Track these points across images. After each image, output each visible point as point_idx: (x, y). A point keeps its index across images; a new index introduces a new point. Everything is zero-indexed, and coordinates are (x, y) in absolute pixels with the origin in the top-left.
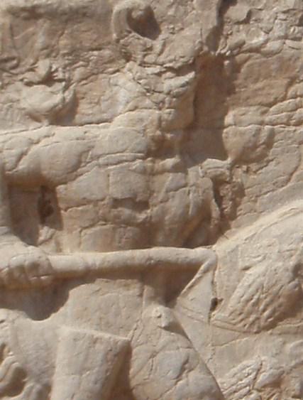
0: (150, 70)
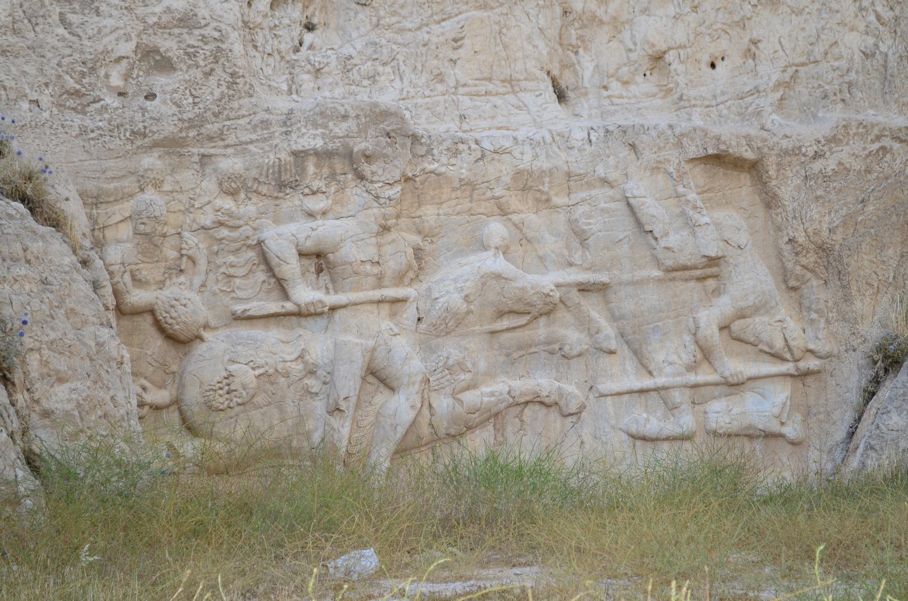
0: (376, 185)
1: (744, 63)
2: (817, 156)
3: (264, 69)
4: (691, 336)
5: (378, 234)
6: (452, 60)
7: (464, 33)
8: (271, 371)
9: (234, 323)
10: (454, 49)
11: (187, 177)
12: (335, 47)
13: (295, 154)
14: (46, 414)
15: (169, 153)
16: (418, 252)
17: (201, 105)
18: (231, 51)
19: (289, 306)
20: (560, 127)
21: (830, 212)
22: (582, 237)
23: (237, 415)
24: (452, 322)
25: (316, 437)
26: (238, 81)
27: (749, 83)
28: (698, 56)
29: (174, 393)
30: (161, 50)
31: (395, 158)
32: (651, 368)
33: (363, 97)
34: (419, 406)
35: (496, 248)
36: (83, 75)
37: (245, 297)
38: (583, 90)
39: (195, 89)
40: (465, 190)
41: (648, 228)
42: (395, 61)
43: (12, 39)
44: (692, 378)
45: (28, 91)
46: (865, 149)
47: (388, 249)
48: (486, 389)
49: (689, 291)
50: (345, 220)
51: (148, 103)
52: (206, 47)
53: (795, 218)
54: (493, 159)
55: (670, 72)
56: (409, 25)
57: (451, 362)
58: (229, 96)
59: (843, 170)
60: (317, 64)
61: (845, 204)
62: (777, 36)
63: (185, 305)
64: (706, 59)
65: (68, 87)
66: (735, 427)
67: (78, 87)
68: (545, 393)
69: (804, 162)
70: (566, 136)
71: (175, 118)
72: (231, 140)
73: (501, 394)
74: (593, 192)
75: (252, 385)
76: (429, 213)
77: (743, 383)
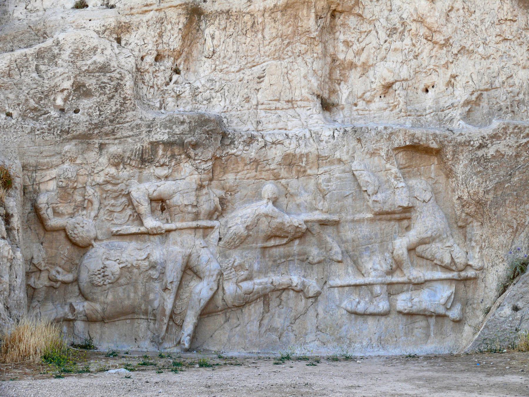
0: (197, 162)
1: (447, 89)
2: (481, 147)
3: (147, 94)
4: (390, 254)
5: (197, 189)
6: (256, 89)
7: (264, 74)
8: (129, 265)
9: (113, 237)
10: (258, 83)
11: (92, 155)
12: (191, 82)
13: (151, 143)
15: (81, 143)
17: (104, 116)
18: (125, 85)
19: (143, 229)
21: (486, 182)
23: (109, 289)
24: (238, 241)
26: (127, 102)
27: (445, 102)
28: (416, 86)
29: (76, 275)
30: (87, 85)
31: (209, 146)
32: (363, 272)
33: (202, 111)
34: (215, 288)
35: (268, 199)
36: (41, 99)
37: (119, 223)
38: (341, 106)
39: (102, 107)
40: (253, 165)
41: (364, 189)
42: (223, 90)
44: (389, 279)
45: (7, 108)
46: (517, 142)
47: (203, 199)
48: (257, 281)
50: (178, 181)
51: (74, 114)
52: (112, 83)
53: (462, 184)
54: (271, 147)
55: (395, 95)
56: (233, 69)
57: (236, 264)
58: (121, 111)
59: (499, 155)
60: (178, 92)
61: (497, 176)
62: (469, 74)
63: (83, 227)
64: (422, 86)
65: (30, 106)
66: (415, 309)
67: (36, 106)
68: (294, 284)
69: (471, 150)
70: (320, 133)
71: (87, 123)
73: (266, 283)
74: (332, 167)
75: (118, 273)
76: (230, 178)
77: (422, 283)
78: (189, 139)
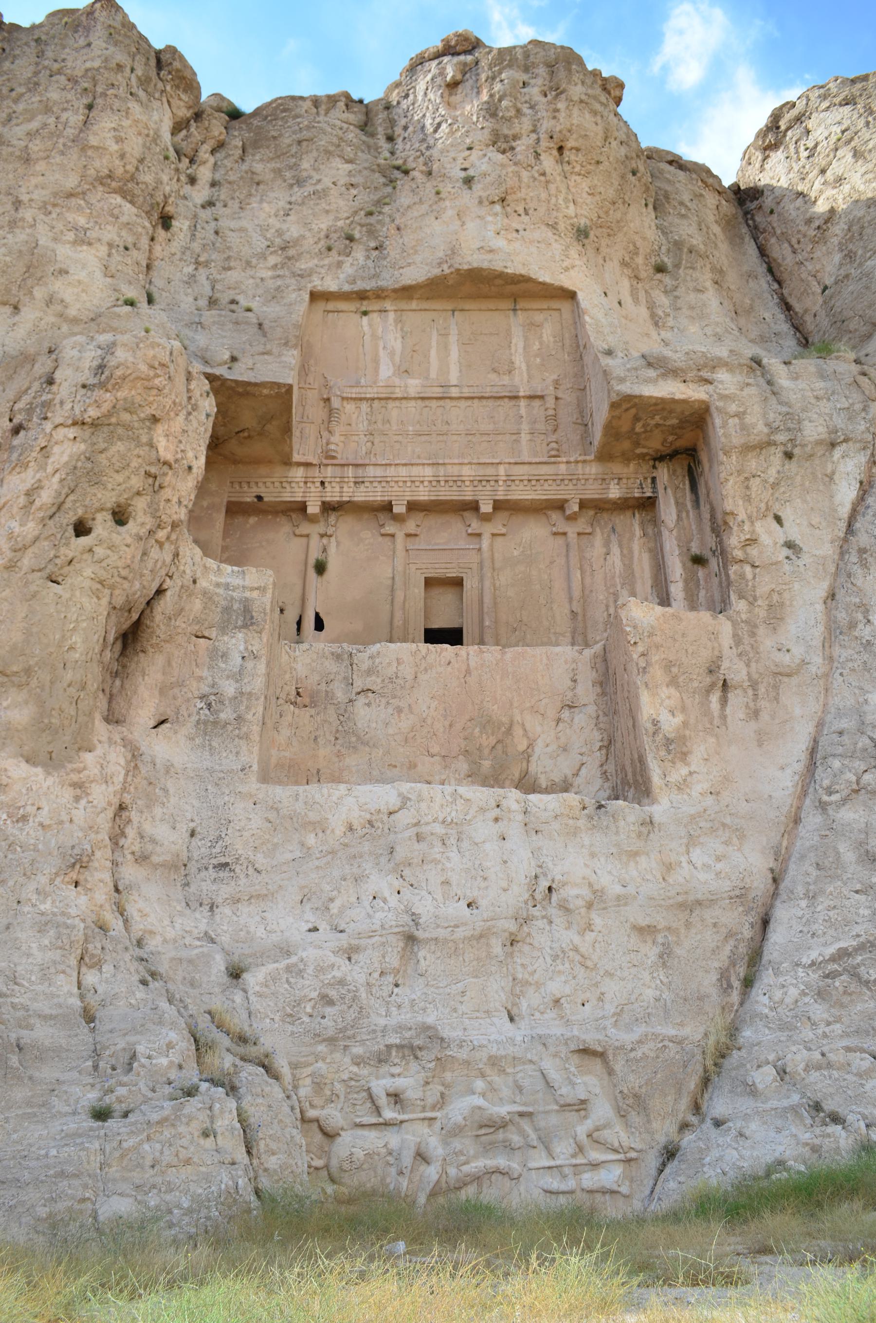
2: (632, 1050)
11: (337, 1056)
13: (387, 1046)
14: (266, 1170)
16: (442, 1095)
19: (381, 1120)
20: (510, 1035)
22: (520, 1089)
25: (392, 1187)
33: (420, 1019)
43: (265, 989)
48: (473, 1165)
49: (572, 1116)
59: (645, 1057)
64: (580, 1002)
66: (595, 1187)
72: (358, 1039)
76: (448, 1076)
78: (417, 1042)
